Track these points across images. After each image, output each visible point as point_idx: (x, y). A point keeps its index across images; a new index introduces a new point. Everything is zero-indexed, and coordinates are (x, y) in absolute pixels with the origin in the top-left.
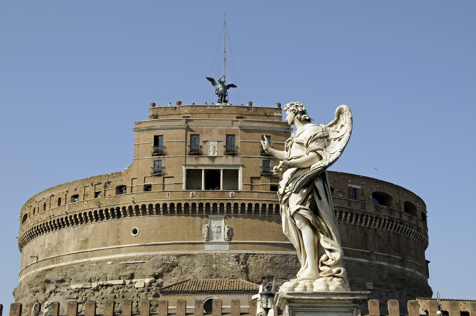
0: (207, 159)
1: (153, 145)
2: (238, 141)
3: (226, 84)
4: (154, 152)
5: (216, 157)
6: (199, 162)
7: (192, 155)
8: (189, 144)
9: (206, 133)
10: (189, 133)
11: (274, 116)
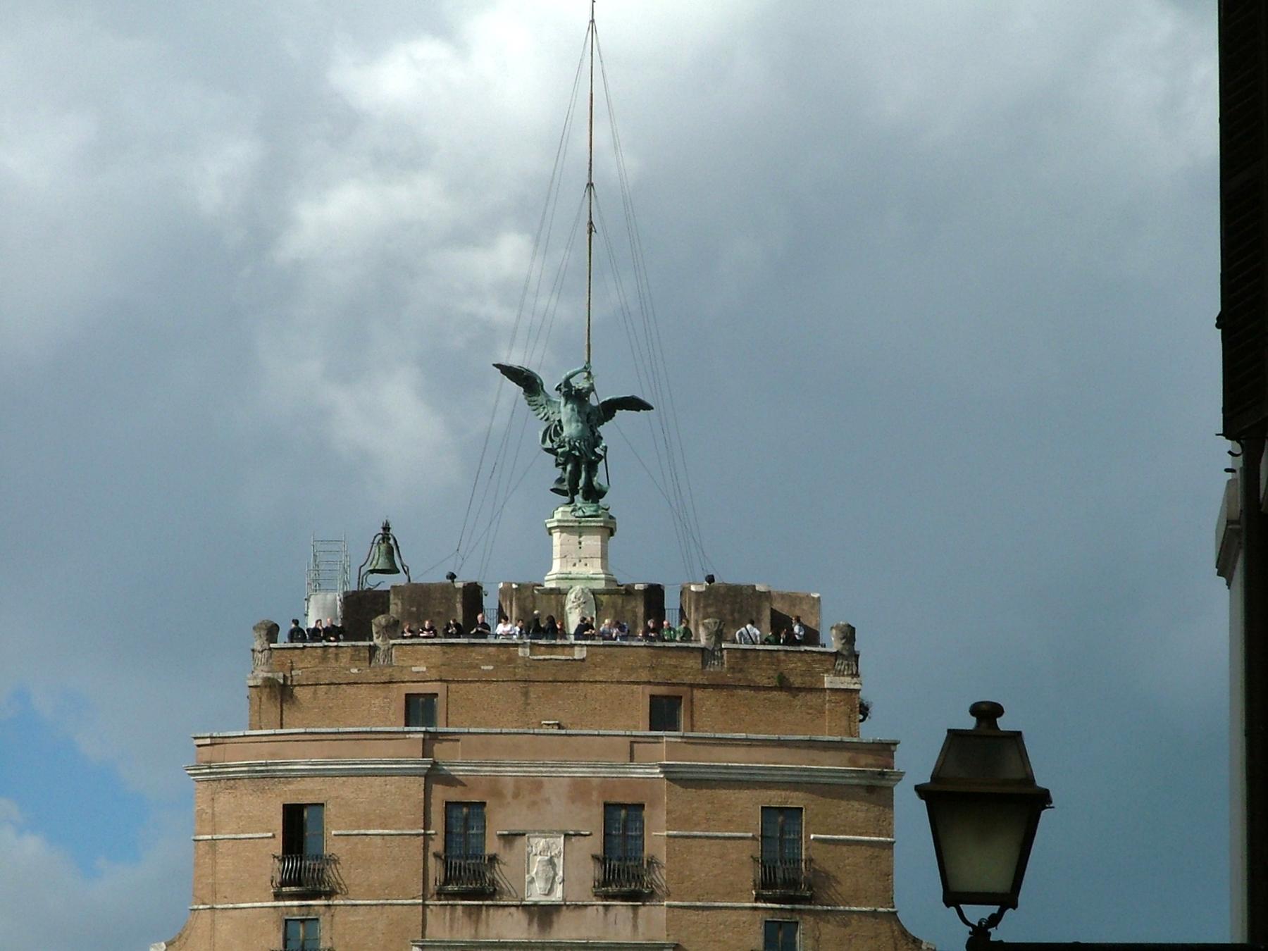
0: (519, 915)
1: (277, 847)
2: (657, 836)
3: (594, 401)
4: (284, 883)
5: (555, 908)
6: (482, 928)
7: (454, 895)
8: (437, 845)
9: (516, 796)
10: (441, 794)
11: (825, 690)
